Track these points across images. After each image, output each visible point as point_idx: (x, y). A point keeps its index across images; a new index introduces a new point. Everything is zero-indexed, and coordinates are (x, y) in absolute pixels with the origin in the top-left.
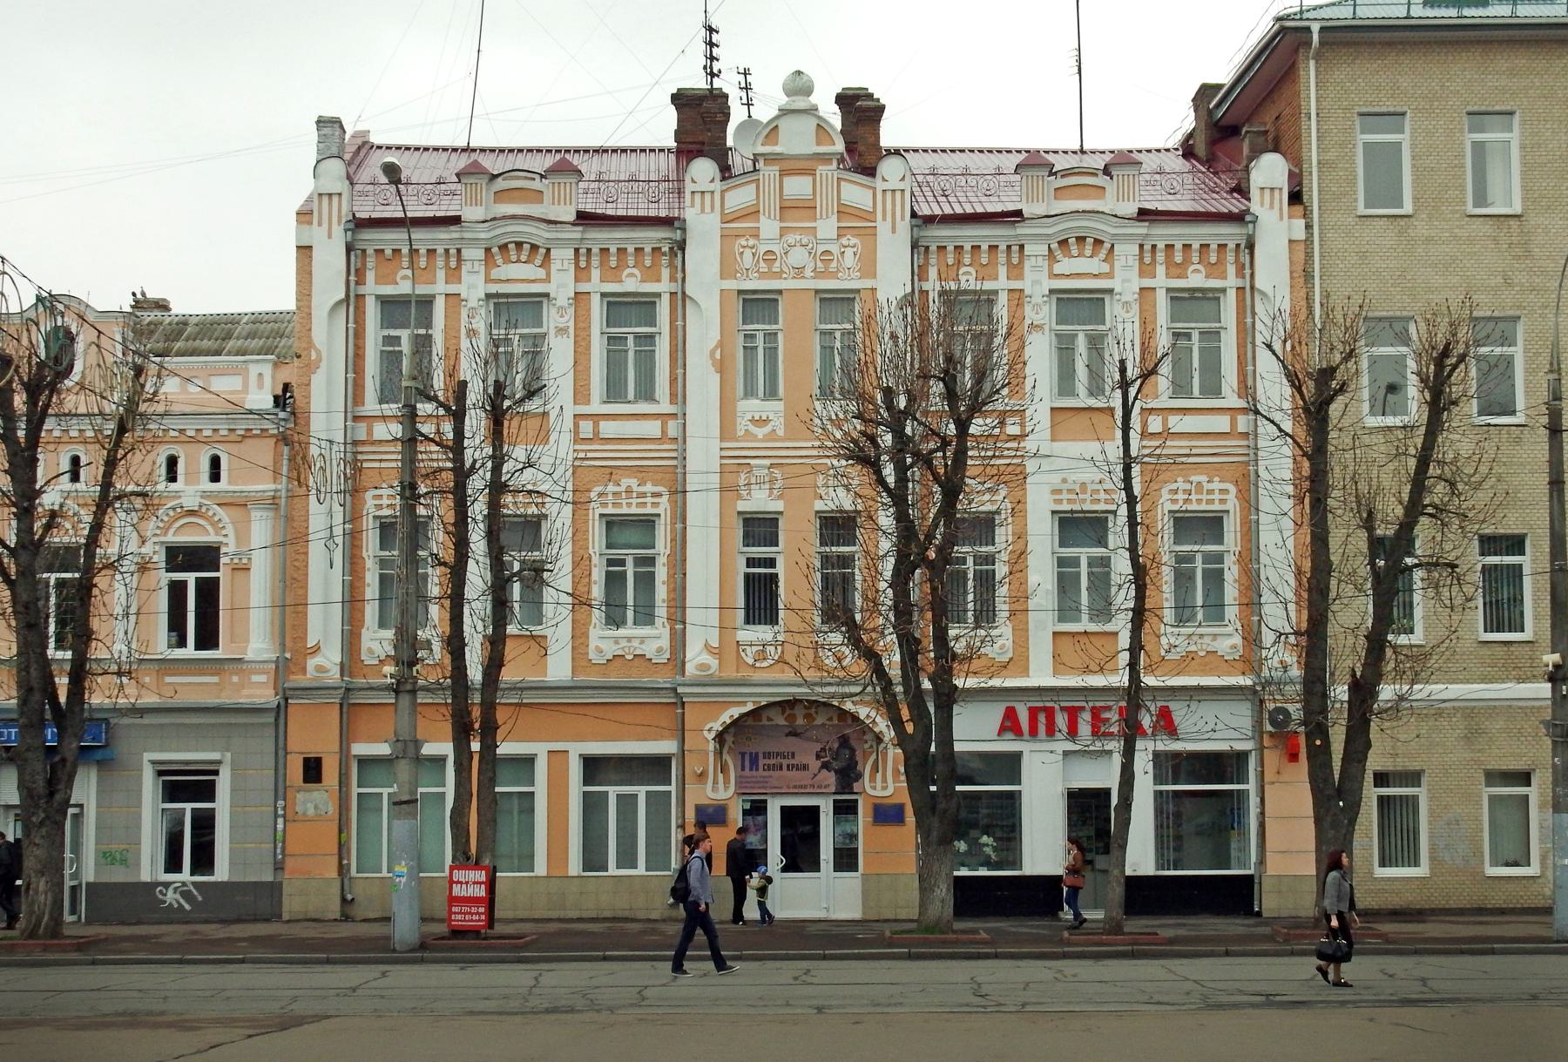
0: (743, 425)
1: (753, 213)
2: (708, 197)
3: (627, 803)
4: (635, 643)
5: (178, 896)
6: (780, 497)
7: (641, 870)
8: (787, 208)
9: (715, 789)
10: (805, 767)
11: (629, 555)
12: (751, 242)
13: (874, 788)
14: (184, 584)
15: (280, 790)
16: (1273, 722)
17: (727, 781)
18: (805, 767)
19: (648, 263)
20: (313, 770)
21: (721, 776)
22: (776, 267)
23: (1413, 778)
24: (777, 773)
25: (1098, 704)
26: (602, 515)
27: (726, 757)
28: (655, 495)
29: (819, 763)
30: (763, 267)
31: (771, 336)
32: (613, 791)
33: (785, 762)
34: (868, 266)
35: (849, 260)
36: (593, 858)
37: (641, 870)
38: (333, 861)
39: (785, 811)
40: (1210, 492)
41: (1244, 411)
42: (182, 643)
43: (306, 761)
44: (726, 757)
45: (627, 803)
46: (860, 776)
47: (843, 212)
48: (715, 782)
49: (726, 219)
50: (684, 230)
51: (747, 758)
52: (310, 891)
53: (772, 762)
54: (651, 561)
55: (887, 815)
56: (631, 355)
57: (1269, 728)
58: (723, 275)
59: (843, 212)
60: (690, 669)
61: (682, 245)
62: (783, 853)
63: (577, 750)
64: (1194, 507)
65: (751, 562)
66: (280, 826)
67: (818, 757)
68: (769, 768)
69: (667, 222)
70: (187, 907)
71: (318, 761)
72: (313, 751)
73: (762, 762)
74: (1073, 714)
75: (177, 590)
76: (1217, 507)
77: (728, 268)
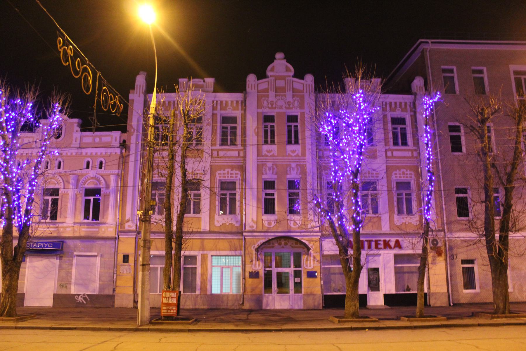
0: (265, 153)
1: (266, 90)
5: (82, 299)
6: (276, 174)
8: (277, 90)
11: (228, 193)
12: (266, 99)
14: (90, 200)
15: (115, 266)
16: (433, 244)
20: (126, 258)
22: (274, 106)
23: (472, 262)
25: (378, 239)
28: (236, 174)
30: (270, 106)
31: (272, 127)
34: (302, 106)
35: (296, 104)
38: (132, 289)
40: (406, 174)
41: (415, 150)
42: (88, 219)
43: (124, 256)
47: (294, 90)
49: (258, 92)
52: (123, 299)
54: (235, 195)
55: (311, 275)
56: (229, 132)
57: (431, 245)
58: (258, 108)
59: (294, 90)
64: (402, 178)
65: (267, 194)
66: (115, 277)
70: (85, 302)
71: (128, 256)
72: (126, 252)
74: (370, 242)
75: (87, 202)
76: (409, 178)
77: (259, 106)
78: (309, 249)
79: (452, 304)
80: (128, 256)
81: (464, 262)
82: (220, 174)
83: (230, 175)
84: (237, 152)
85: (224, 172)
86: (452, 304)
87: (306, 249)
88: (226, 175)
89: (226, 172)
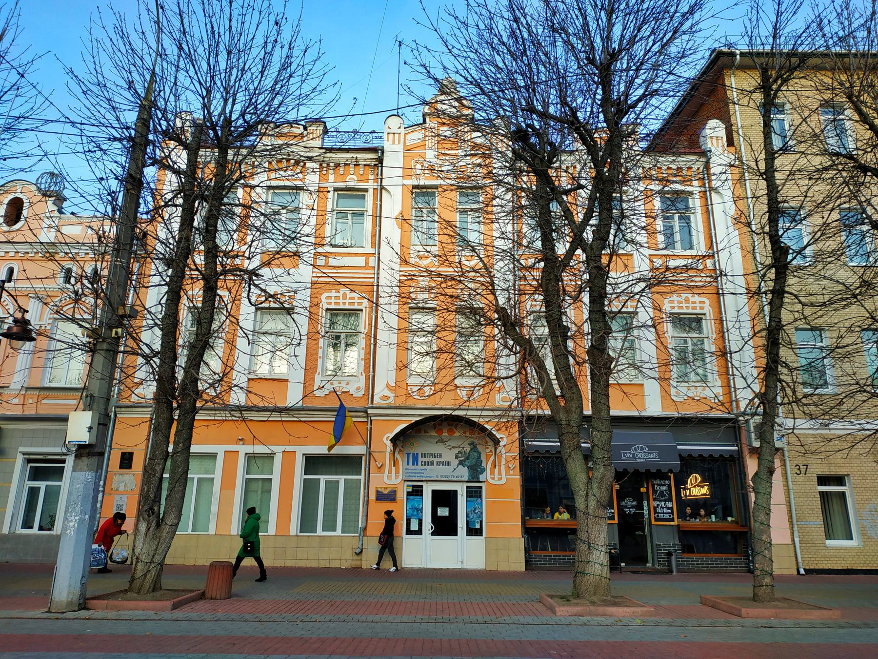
2: (397, 136)
3: (332, 487)
4: (343, 384)
7: (338, 532)
9: (389, 478)
10: (448, 464)
13: (493, 479)
17: (397, 472)
18: (448, 464)
19: (361, 172)
21: (393, 468)
23: (839, 480)
24: (430, 467)
26: (327, 310)
27: (397, 455)
29: (457, 462)
32: (323, 479)
33: (435, 460)
36: (307, 523)
37: (338, 532)
39: (434, 492)
43: (123, 454)
44: (397, 455)
45: (332, 487)
46: (483, 470)
48: (390, 472)
50: (383, 152)
51: (411, 456)
53: (426, 459)
60: (377, 400)
61: (380, 161)
62: (432, 522)
63: (301, 450)
67: (457, 457)
68: (426, 463)
69: (374, 150)
71: (131, 455)
73: (420, 459)
78: (496, 442)
79: (802, 571)
80: (131, 455)
81: (823, 480)
82: (330, 297)
83: (347, 301)
84: (364, 258)
85: (337, 295)
86: (802, 571)
87: (491, 443)
88: (341, 301)
89: (340, 295)
